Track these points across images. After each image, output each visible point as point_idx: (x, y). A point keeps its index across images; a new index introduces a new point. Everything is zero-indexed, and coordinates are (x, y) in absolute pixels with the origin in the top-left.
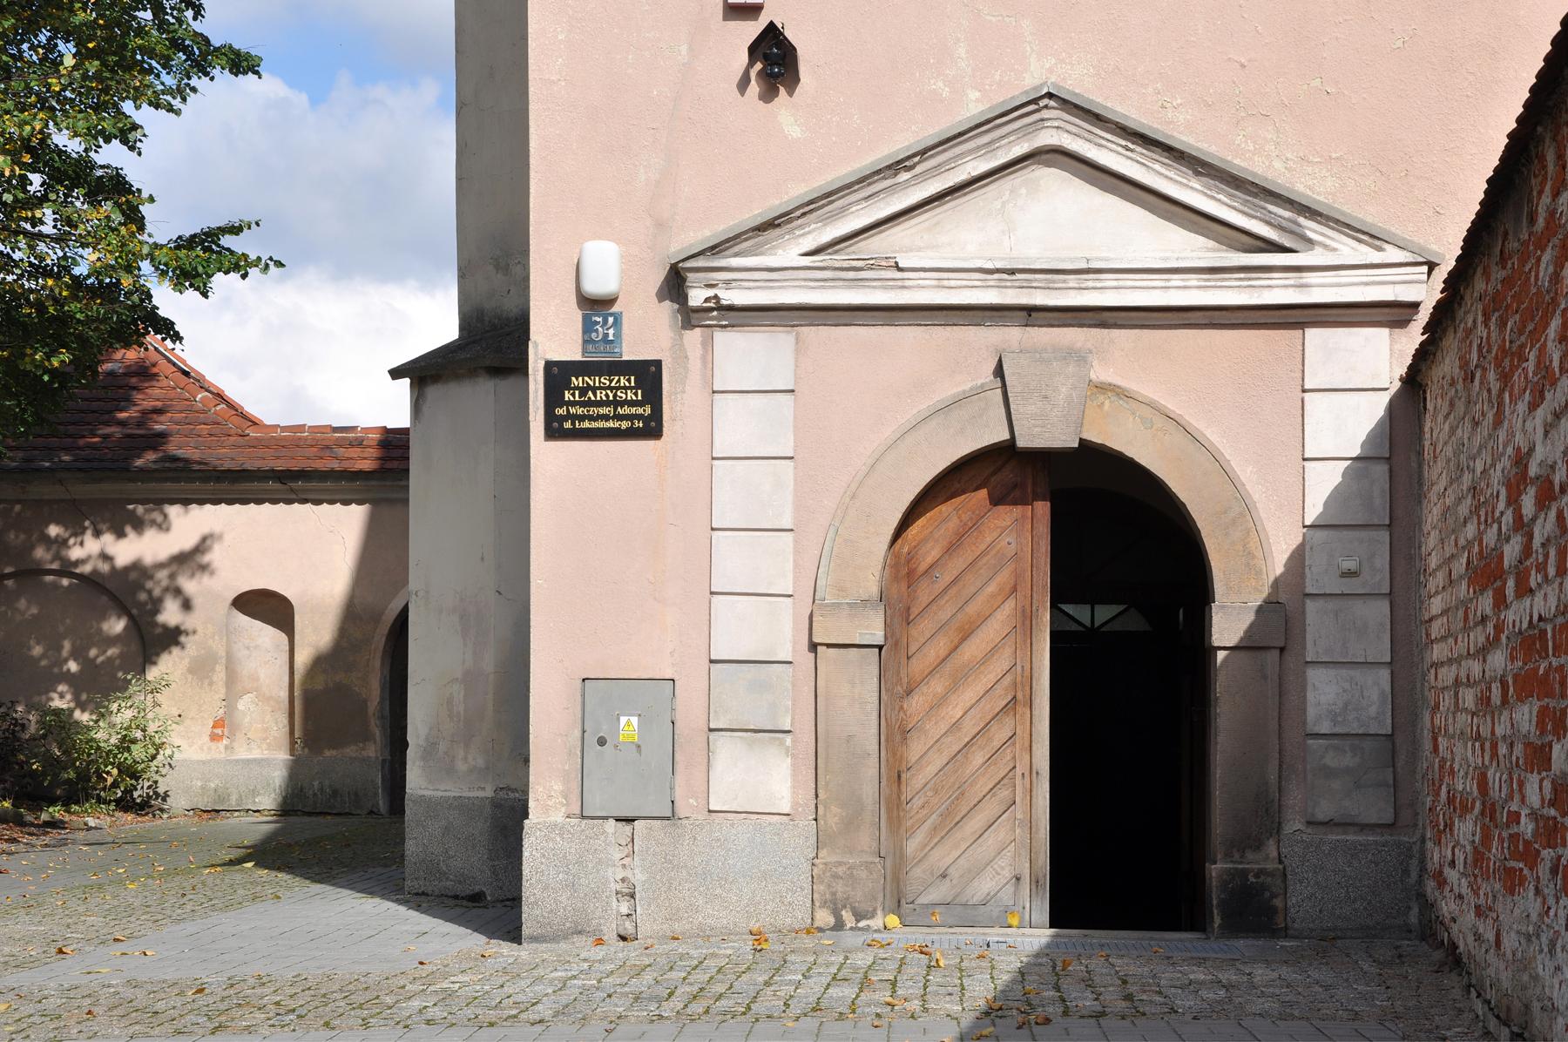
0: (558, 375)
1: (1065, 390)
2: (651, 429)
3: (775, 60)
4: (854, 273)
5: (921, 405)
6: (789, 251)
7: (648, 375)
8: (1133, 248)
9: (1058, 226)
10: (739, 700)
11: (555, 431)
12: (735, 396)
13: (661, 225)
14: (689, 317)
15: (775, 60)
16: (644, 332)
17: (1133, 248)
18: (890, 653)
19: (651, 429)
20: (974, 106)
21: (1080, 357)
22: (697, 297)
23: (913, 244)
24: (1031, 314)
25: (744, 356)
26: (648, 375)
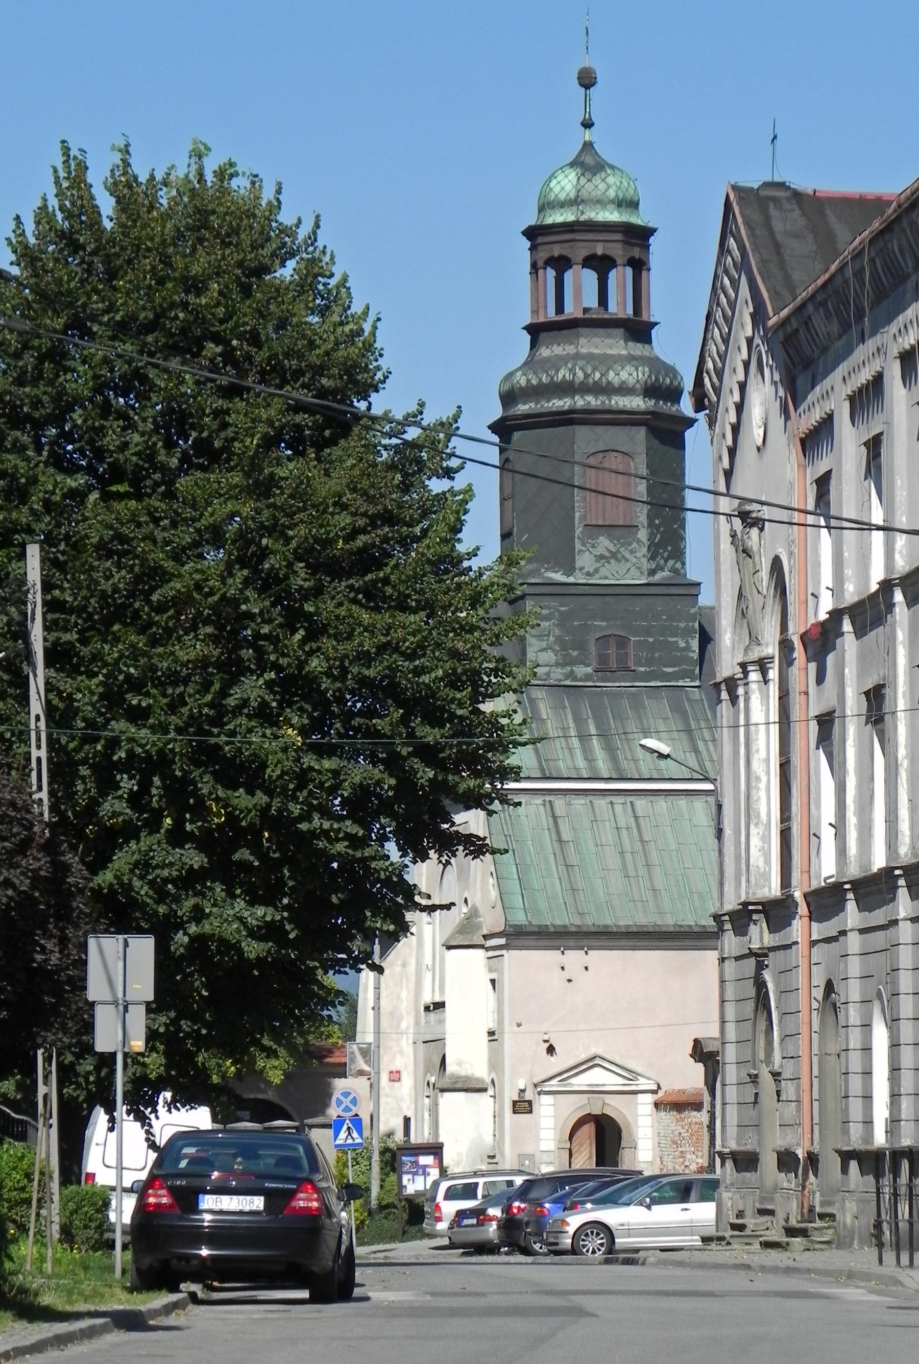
2: (531, 1112)
3: (551, 1050)
4: (565, 1086)
5: (573, 1108)
6: (554, 1082)
7: (530, 1103)
9: (596, 1077)
10: (545, 1158)
13: (532, 1077)
15: (551, 1050)
16: (528, 1096)
18: (570, 1150)
19: (531, 1112)
23: (574, 1081)
25: (545, 1099)
26: (530, 1103)
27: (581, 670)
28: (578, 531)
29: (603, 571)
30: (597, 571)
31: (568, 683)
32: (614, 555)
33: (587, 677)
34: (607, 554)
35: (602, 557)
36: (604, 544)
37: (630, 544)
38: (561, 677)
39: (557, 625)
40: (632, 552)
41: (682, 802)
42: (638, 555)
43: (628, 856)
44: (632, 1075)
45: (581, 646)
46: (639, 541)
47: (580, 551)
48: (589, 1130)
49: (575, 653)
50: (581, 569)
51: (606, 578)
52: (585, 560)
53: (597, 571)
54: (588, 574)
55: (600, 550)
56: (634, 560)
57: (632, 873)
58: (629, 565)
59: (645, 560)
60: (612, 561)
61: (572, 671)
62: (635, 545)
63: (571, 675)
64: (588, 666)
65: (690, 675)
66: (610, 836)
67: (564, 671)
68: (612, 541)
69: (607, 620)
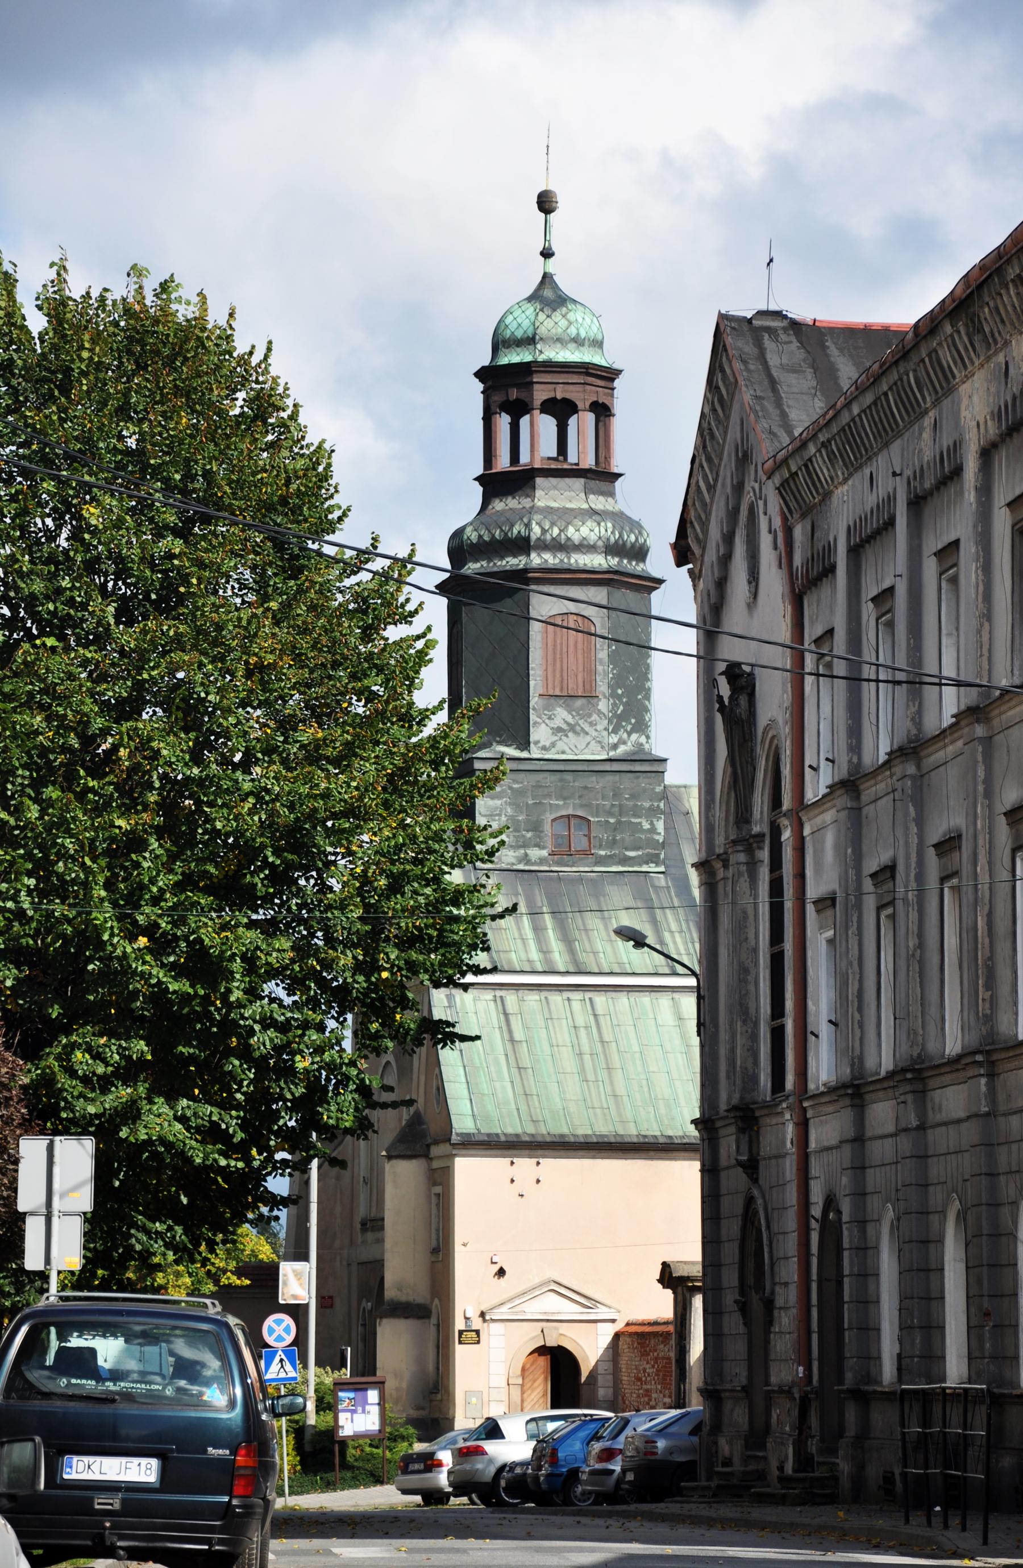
0: (461, 1332)
1: (555, 1335)
2: (478, 1342)
6: (504, 1309)
8: (568, 1309)
11: (460, 1342)
12: (494, 1335)
14: (485, 1321)
16: (477, 1324)
17: (568, 1309)
19: (478, 1342)
20: (537, 1281)
21: (556, 1329)
22: (487, 1317)
24: (548, 1321)
26: (477, 1332)
27: (535, 853)
28: (534, 701)
29: (561, 745)
30: (553, 744)
31: (521, 867)
32: (572, 728)
33: (542, 861)
34: (564, 726)
35: (559, 730)
36: (562, 715)
37: (590, 716)
38: (513, 861)
39: (510, 804)
40: (591, 724)
41: (645, 999)
42: (598, 727)
43: (587, 1058)
44: (589, 1302)
45: (536, 827)
46: (599, 712)
47: (535, 723)
48: (543, 1362)
49: (529, 835)
50: (536, 743)
51: (563, 752)
52: (540, 733)
53: (553, 744)
54: (544, 748)
55: (558, 722)
56: (594, 734)
57: (591, 1077)
58: (588, 738)
59: (605, 733)
60: (570, 734)
61: (526, 855)
62: (595, 717)
63: (526, 859)
64: (544, 848)
65: (654, 859)
66: (567, 1035)
67: (517, 854)
68: (570, 713)
69: (564, 799)
